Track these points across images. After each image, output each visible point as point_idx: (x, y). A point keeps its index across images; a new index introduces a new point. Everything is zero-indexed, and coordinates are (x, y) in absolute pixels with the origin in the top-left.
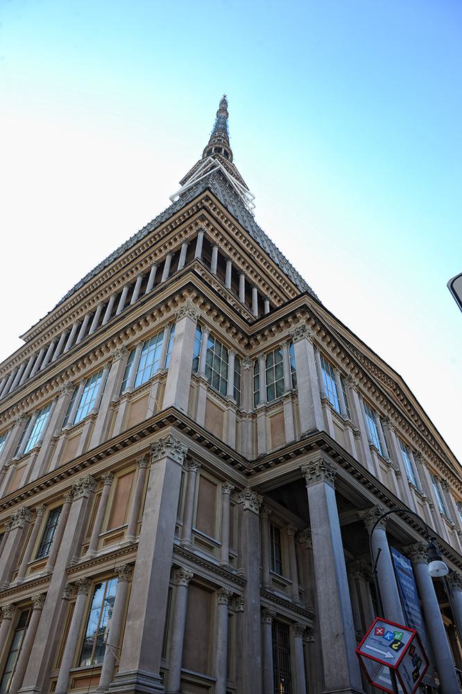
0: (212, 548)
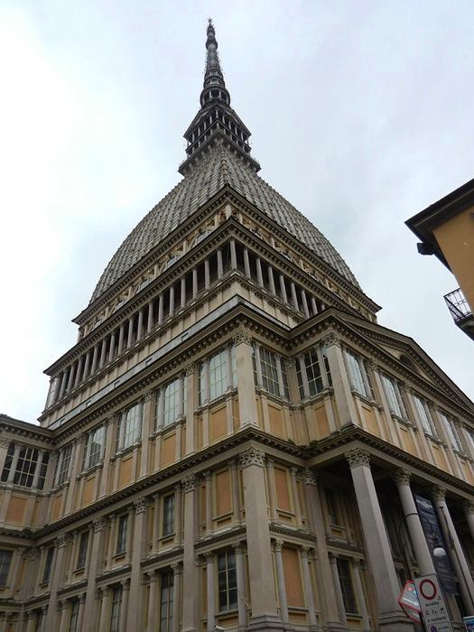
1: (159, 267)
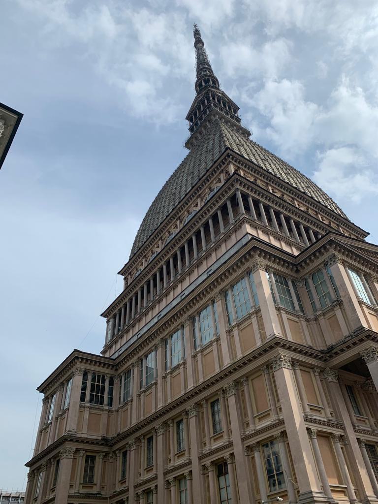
0: (320, 411)
1: (181, 222)
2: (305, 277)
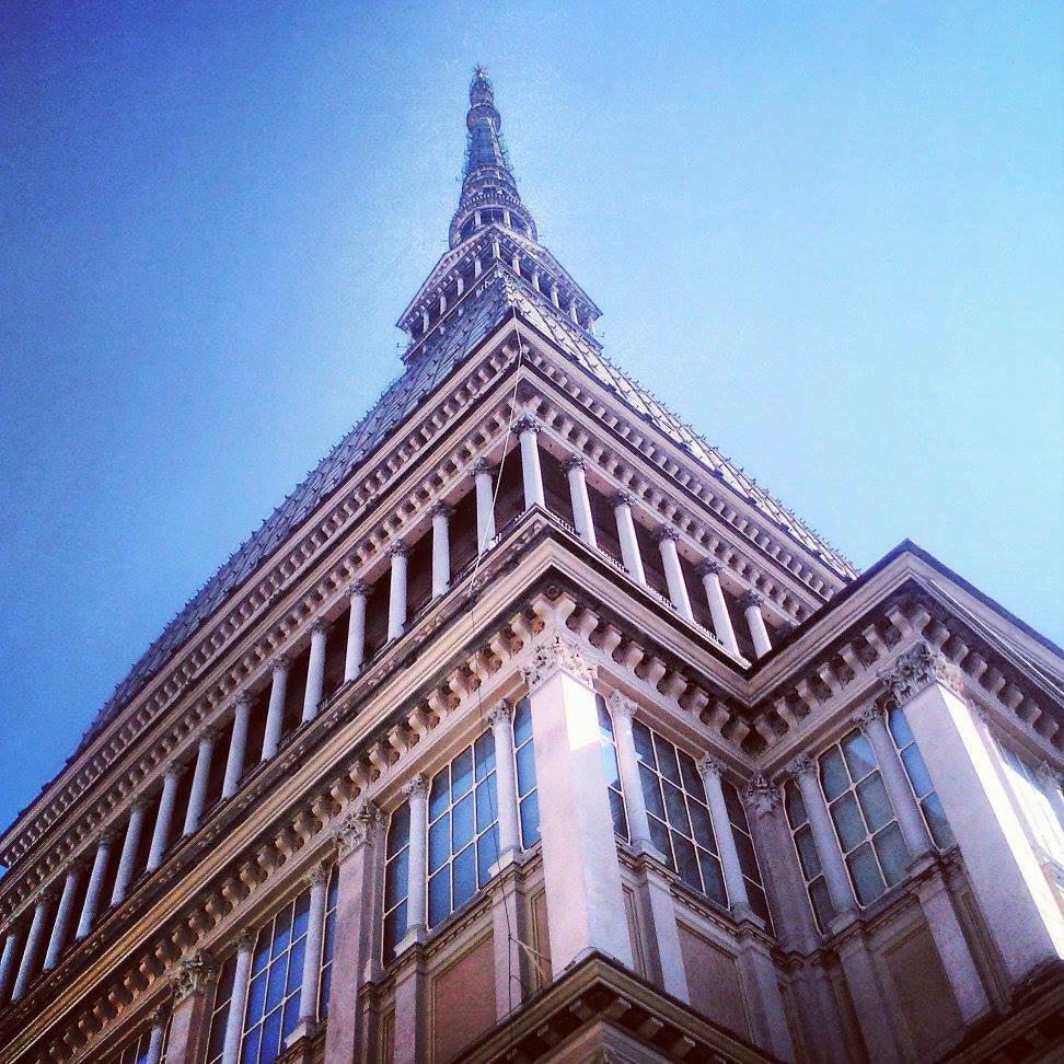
2: (789, 767)
